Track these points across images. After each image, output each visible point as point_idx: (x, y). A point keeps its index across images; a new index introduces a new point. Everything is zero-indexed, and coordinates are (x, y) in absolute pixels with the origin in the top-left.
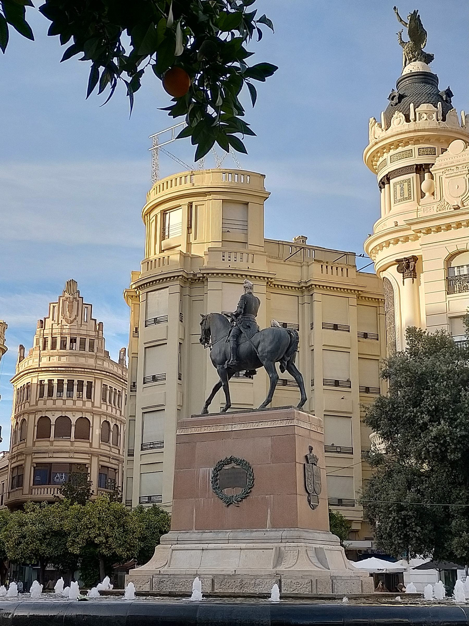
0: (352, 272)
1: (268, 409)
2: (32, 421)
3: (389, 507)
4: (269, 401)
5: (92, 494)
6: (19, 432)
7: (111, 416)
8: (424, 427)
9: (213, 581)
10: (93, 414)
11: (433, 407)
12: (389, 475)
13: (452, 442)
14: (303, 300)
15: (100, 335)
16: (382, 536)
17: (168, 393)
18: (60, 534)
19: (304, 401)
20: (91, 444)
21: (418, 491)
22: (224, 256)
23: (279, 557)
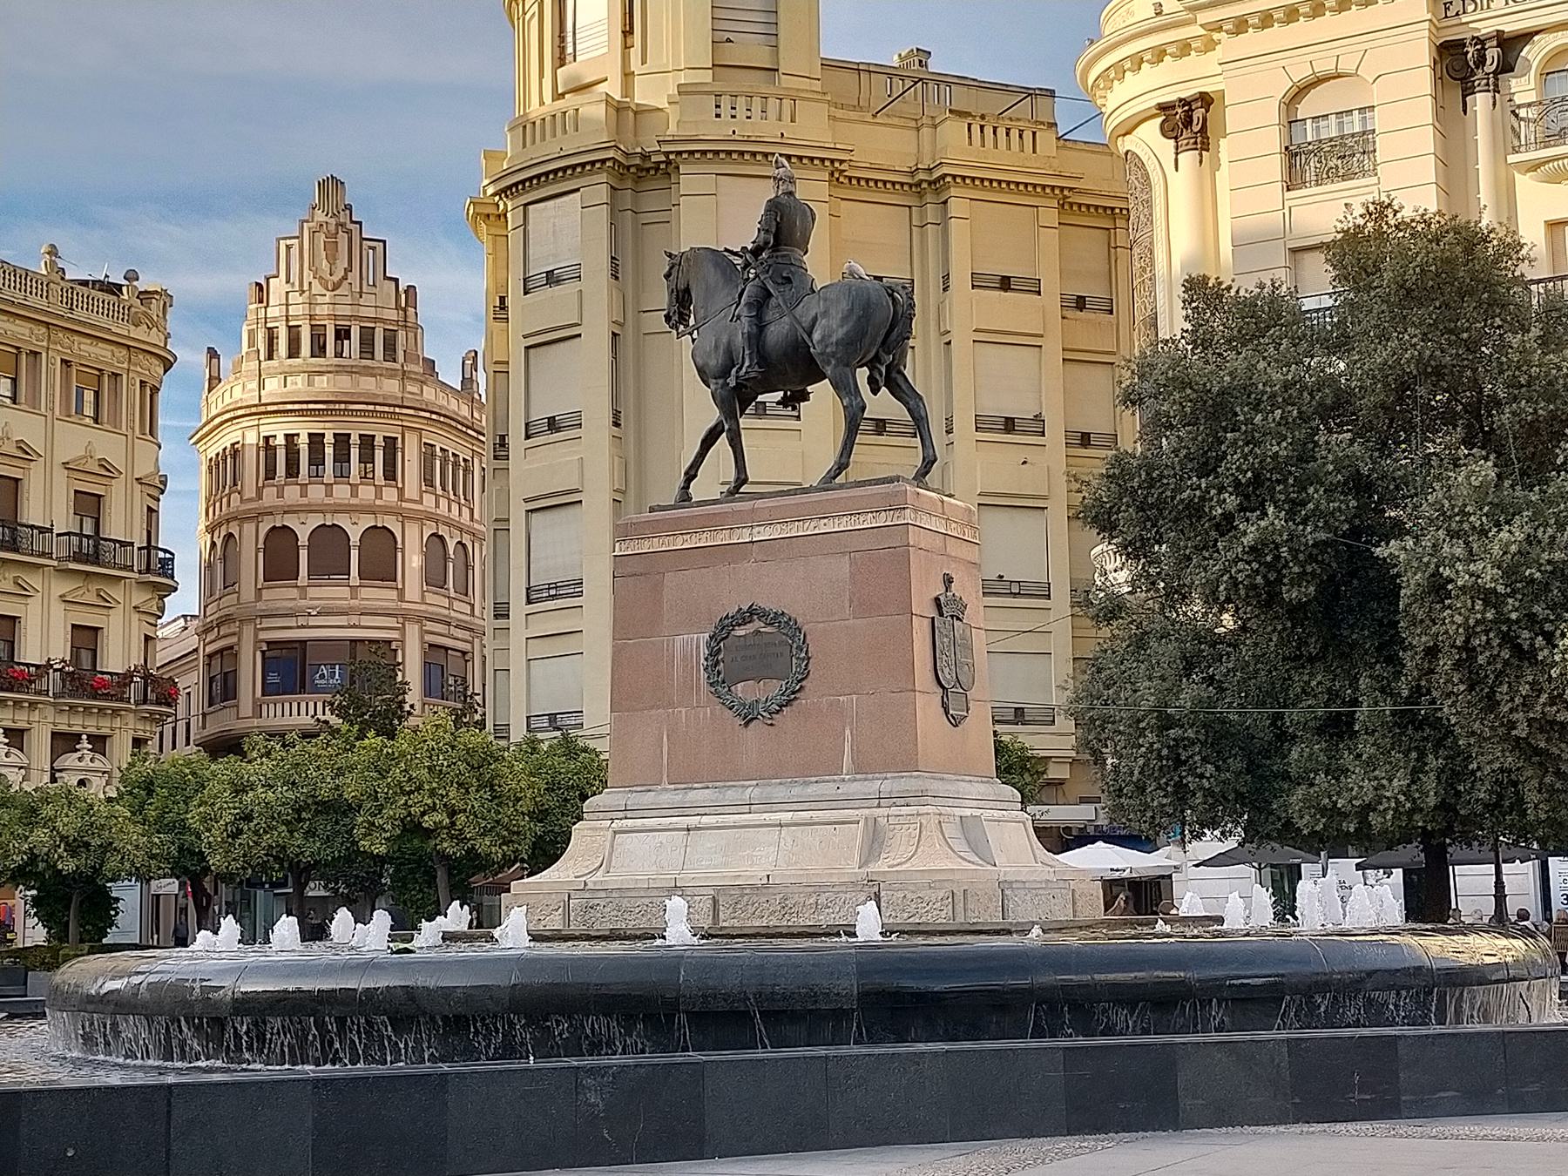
0: (1046, 139)
1: (841, 486)
2: (251, 539)
3: (1139, 721)
4: (842, 466)
5: (409, 713)
6: (219, 567)
7: (449, 523)
8: (1226, 525)
9: (715, 901)
10: (404, 517)
11: (1249, 474)
12: (1140, 643)
13: (1295, 558)
14: (922, 216)
15: (411, 319)
16: (1121, 790)
17: (588, 458)
18: (336, 809)
19: (929, 462)
20: (401, 592)
21: (1210, 680)
22: (718, 106)
23: (875, 842)
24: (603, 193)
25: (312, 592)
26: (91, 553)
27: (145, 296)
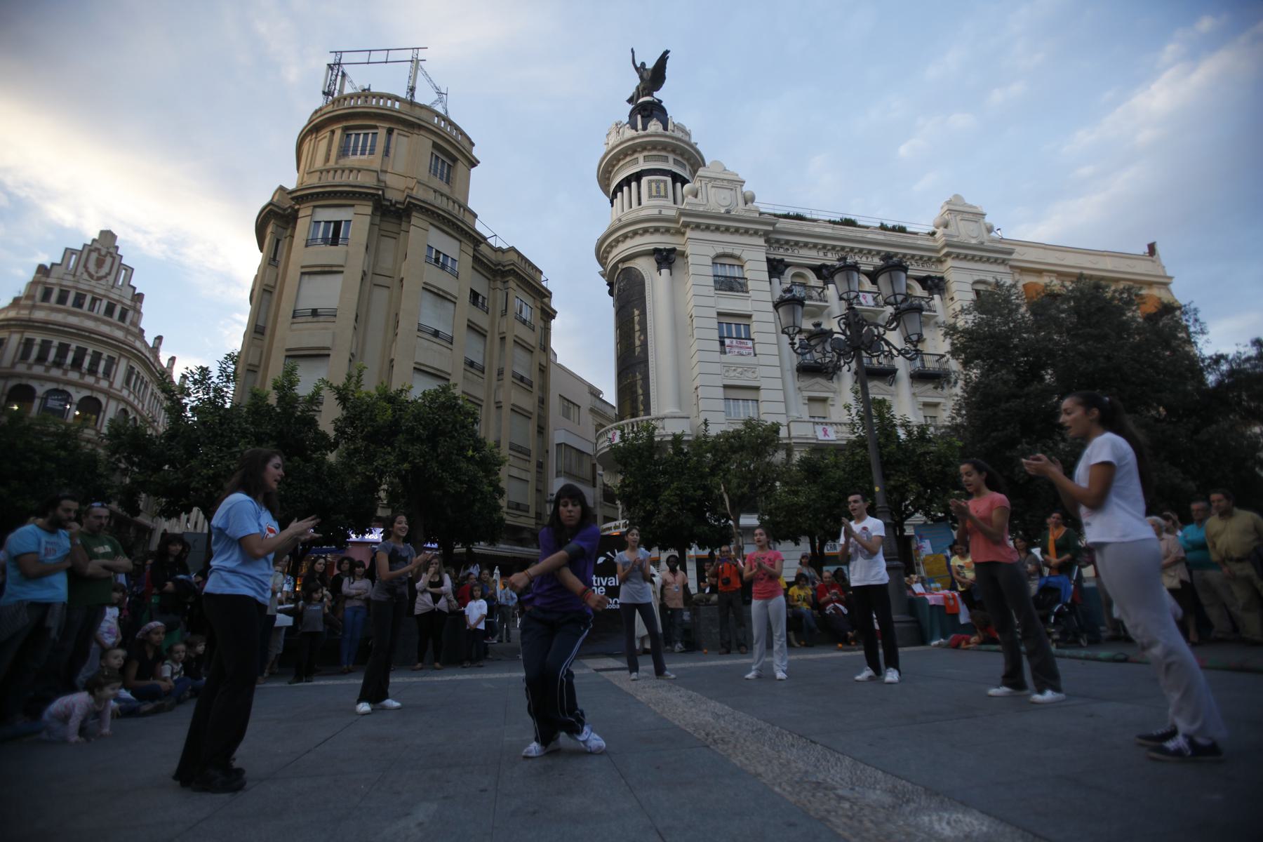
10: (110, 396)
24: (369, 210)
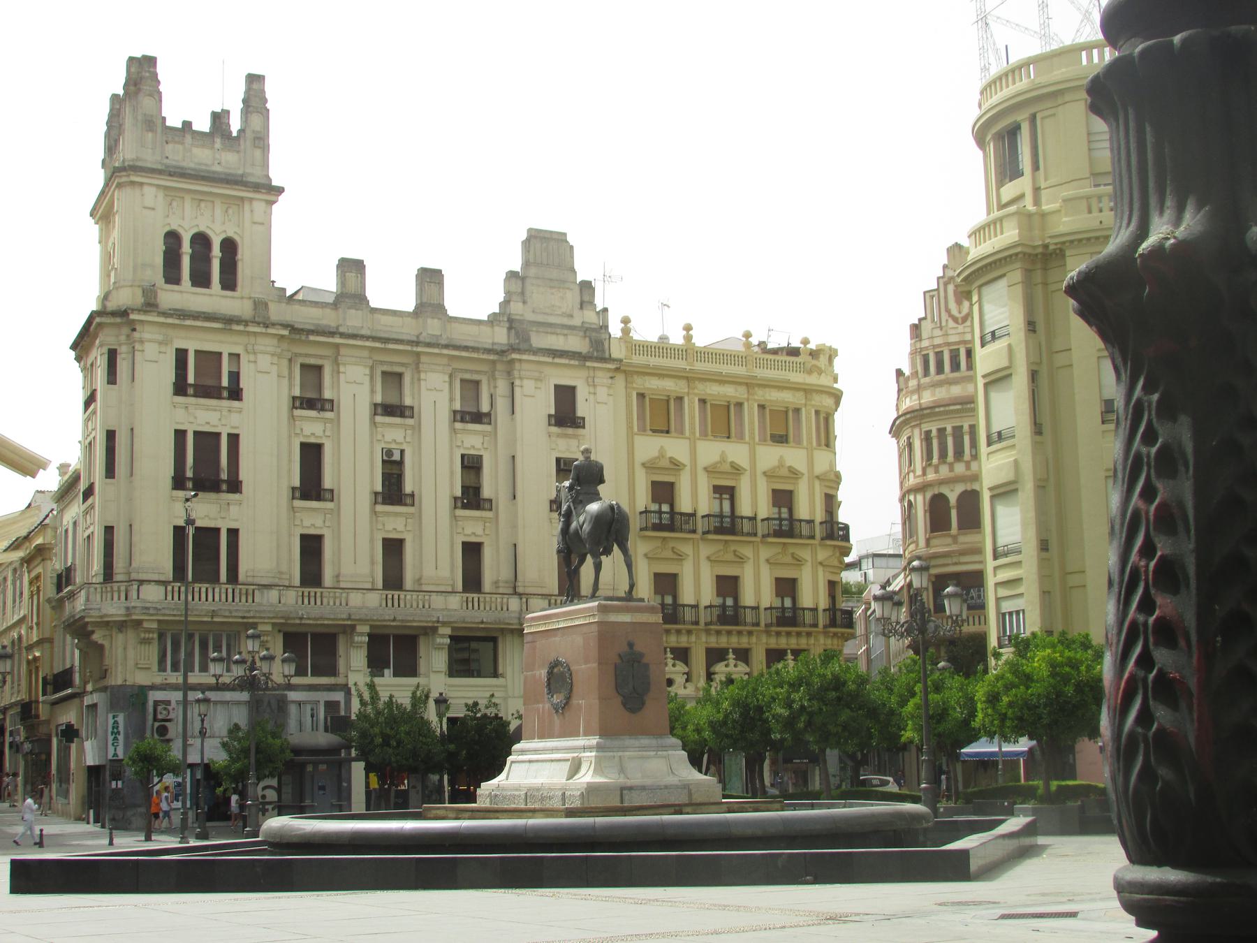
2: (920, 501)
24: (1017, 276)
25: (962, 539)
26: (787, 528)
27: (814, 354)
